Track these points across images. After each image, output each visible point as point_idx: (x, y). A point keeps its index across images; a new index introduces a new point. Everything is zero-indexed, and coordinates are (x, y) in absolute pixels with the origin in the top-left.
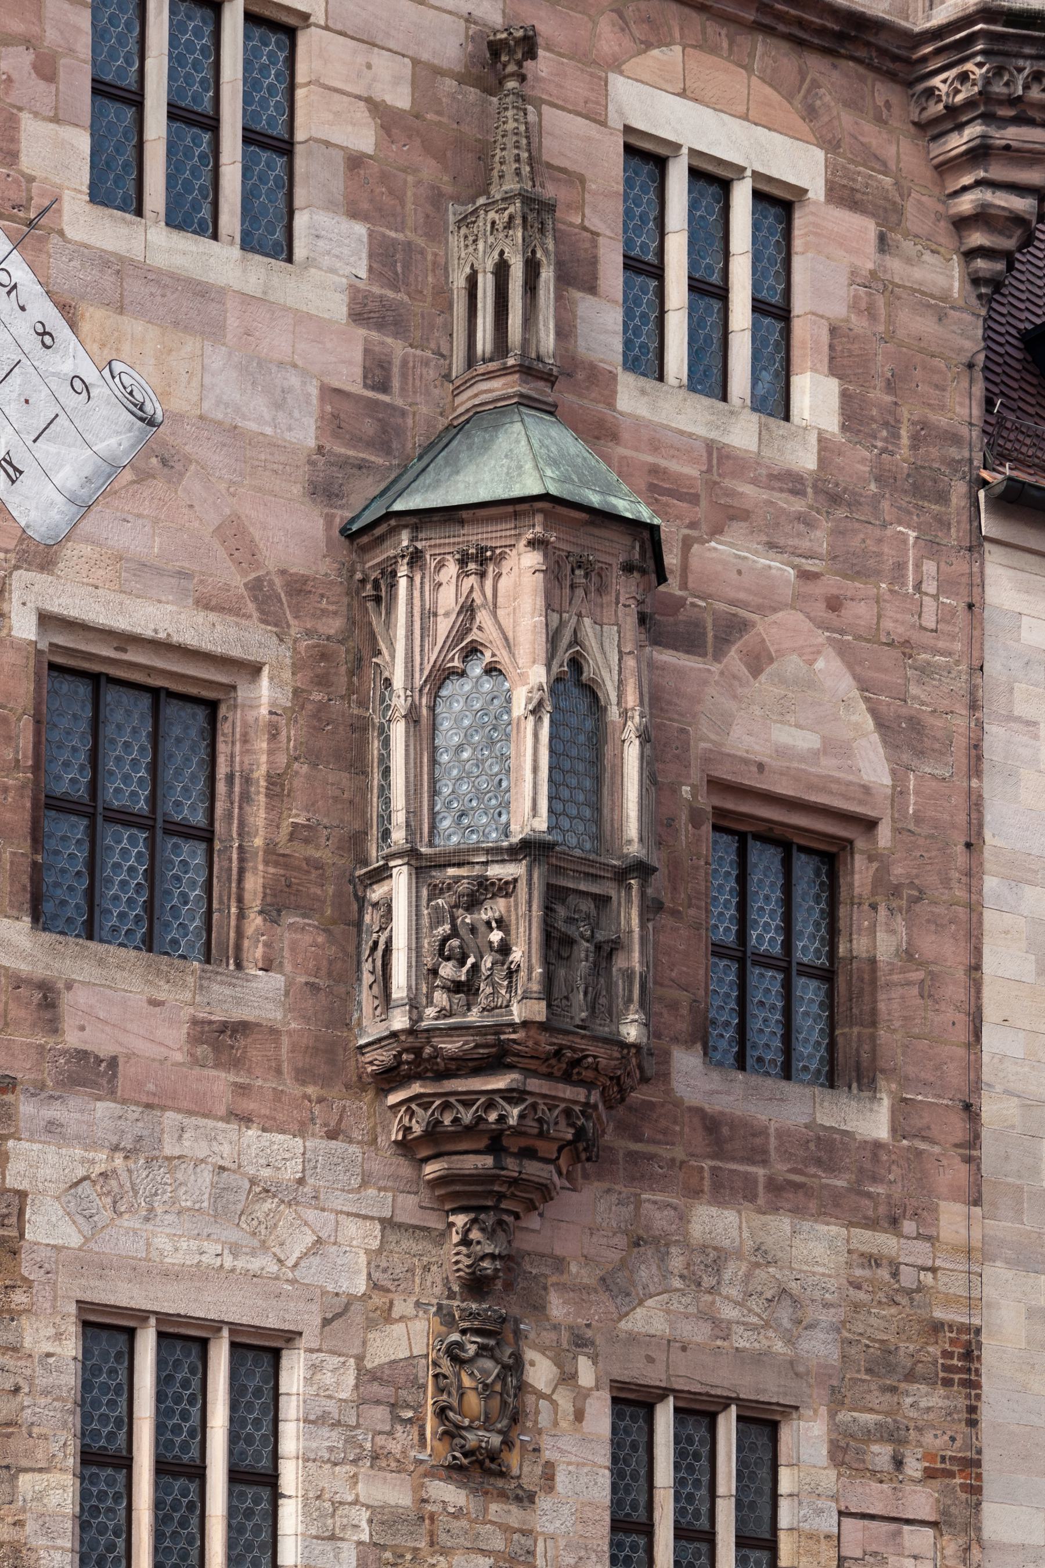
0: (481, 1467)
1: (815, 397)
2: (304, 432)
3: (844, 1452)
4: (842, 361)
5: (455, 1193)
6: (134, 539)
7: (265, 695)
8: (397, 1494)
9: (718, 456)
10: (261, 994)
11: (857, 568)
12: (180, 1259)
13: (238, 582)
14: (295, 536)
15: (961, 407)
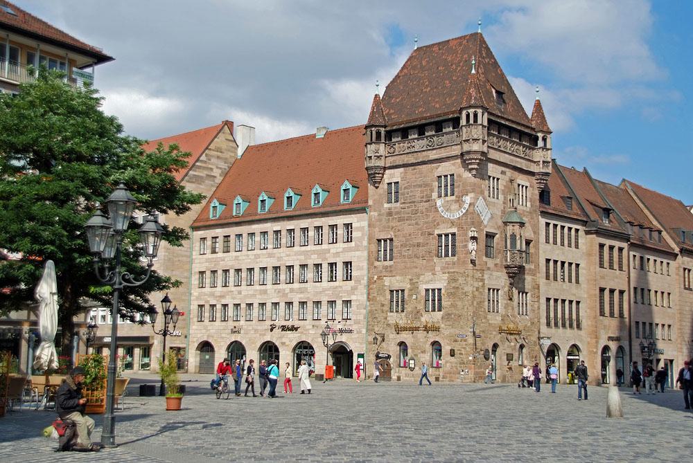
0: (511, 299)
1: (529, 204)
2: (500, 213)
3: (532, 297)
4: (531, 201)
5: (510, 277)
6: (491, 224)
7: (497, 236)
8: (505, 302)
9: (524, 211)
10: (498, 261)
11: (532, 218)
12: (494, 284)
13: (496, 227)
14: (500, 223)
15: (538, 203)
